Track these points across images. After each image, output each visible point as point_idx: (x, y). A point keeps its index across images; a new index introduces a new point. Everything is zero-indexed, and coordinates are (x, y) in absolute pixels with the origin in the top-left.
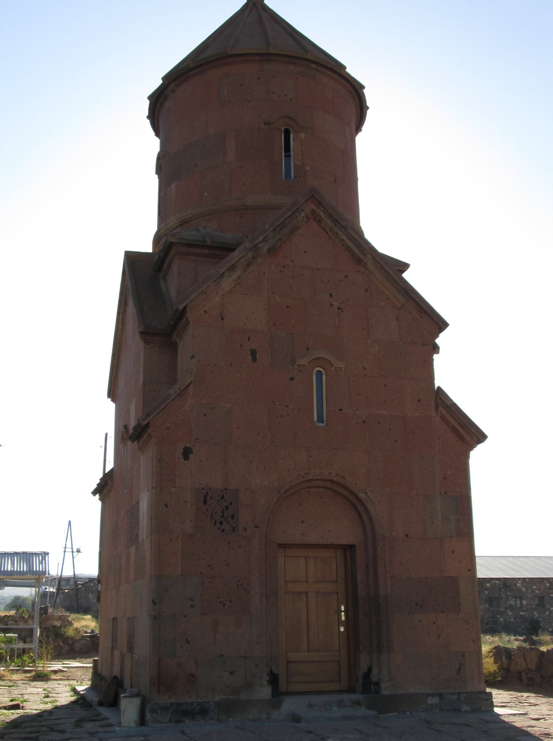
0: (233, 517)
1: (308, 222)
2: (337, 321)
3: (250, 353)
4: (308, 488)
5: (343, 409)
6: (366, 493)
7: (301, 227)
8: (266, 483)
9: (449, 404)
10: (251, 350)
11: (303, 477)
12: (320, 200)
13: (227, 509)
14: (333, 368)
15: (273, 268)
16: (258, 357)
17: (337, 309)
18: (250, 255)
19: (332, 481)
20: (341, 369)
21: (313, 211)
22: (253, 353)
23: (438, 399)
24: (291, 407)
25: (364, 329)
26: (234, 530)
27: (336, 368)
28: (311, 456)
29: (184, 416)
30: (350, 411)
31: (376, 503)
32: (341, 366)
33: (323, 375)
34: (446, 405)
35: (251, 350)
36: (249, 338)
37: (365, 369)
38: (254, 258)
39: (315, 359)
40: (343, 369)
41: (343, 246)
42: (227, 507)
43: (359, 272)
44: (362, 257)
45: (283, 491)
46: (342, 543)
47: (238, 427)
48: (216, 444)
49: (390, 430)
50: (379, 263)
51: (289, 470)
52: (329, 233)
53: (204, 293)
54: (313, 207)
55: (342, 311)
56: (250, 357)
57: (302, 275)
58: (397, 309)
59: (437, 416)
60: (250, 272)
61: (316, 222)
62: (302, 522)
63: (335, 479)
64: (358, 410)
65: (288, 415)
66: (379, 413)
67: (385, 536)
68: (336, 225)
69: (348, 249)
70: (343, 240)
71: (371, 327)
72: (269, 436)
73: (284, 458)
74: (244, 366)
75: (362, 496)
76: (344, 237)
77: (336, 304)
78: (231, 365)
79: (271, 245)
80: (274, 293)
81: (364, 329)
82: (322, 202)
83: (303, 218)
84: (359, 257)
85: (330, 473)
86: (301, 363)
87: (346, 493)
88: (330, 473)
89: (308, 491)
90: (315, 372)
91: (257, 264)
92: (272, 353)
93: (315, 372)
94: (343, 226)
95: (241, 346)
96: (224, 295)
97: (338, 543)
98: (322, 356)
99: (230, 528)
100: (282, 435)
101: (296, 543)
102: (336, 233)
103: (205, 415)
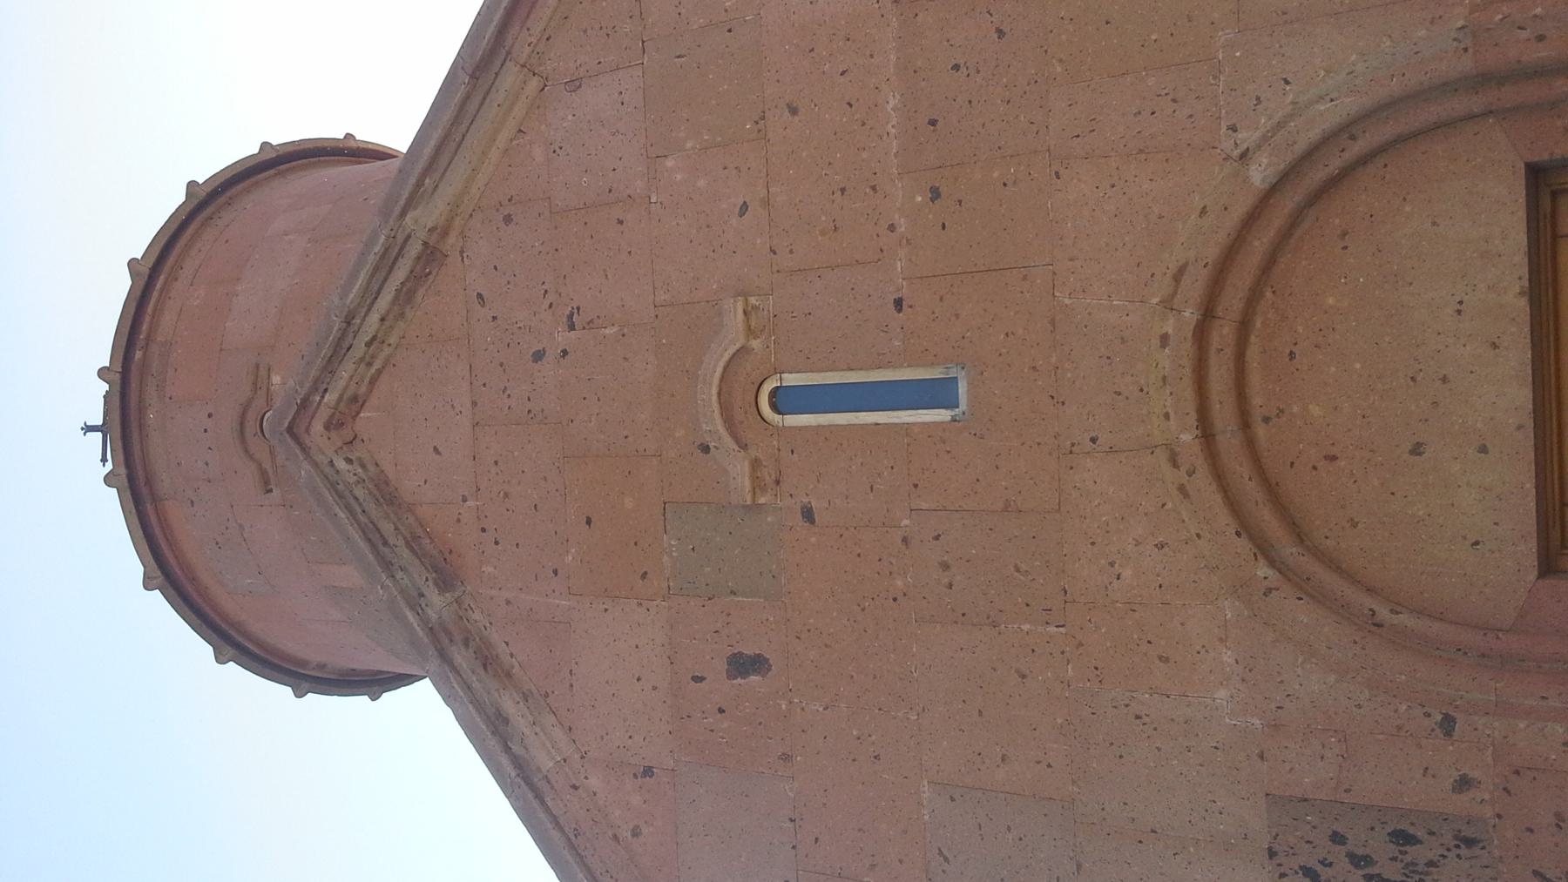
0: (1402, 838)
1: (363, 441)
2: (607, 331)
3: (739, 681)
4: (1245, 424)
6: (1243, 156)
7: (377, 464)
8: (1228, 657)
10: (731, 676)
11: (1190, 473)
13: (1367, 860)
14: (755, 344)
15: (491, 569)
16: (749, 650)
18: (461, 657)
19: (1208, 313)
20: (755, 308)
21: (327, 427)
22: (743, 665)
24: (906, 522)
26: (1470, 842)
27: (750, 332)
28: (1093, 440)
30: (900, 260)
31: (1290, 97)
33: (784, 385)
35: (731, 676)
36: (698, 679)
37: (744, 208)
38: (466, 643)
40: (753, 300)
41: (402, 315)
42: (1356, 860)
43: (462, 252)
44: (415, 248)
45: (1263, 570)
46: (1519, 238)
48: (1079, 866)
49: (956, 67)
51: (1160, 546)
52: (377, 365)
54: (318, 426)
56: (752, 677)
58: (546, 88)
60: (512, 655)
61: (358, 413)
62: (1417, 450)
63: (1190, 315)
64: (892, 228)
65: (937, 538)
67: (1463, 27)
68: (348, 349)
69: (406, 296)
70: (382, 320)
72: (1026, 627)
73: (1112, 564)
74: (784, 707)
75: (1260, 174)
76: (374, 318)
78: (786, 758)
79: (427, 580)
80: (556, 572)
81: (621, 222)
83: (349, 461)
85: (1164, 339)
86: (747, 483)
87: (1259, 244)
88: (1164, 339)
89: (1266, 420)
90: (775, 418)
92: (733, 593)
93: (775, 418)
95: (721, 711)
96: (582, 757)
97: (1520, 259)
98: (715, 398)
99: (1459, 856)
100: (1018, 570)
101: (1530, 486)
102: (368, 345)
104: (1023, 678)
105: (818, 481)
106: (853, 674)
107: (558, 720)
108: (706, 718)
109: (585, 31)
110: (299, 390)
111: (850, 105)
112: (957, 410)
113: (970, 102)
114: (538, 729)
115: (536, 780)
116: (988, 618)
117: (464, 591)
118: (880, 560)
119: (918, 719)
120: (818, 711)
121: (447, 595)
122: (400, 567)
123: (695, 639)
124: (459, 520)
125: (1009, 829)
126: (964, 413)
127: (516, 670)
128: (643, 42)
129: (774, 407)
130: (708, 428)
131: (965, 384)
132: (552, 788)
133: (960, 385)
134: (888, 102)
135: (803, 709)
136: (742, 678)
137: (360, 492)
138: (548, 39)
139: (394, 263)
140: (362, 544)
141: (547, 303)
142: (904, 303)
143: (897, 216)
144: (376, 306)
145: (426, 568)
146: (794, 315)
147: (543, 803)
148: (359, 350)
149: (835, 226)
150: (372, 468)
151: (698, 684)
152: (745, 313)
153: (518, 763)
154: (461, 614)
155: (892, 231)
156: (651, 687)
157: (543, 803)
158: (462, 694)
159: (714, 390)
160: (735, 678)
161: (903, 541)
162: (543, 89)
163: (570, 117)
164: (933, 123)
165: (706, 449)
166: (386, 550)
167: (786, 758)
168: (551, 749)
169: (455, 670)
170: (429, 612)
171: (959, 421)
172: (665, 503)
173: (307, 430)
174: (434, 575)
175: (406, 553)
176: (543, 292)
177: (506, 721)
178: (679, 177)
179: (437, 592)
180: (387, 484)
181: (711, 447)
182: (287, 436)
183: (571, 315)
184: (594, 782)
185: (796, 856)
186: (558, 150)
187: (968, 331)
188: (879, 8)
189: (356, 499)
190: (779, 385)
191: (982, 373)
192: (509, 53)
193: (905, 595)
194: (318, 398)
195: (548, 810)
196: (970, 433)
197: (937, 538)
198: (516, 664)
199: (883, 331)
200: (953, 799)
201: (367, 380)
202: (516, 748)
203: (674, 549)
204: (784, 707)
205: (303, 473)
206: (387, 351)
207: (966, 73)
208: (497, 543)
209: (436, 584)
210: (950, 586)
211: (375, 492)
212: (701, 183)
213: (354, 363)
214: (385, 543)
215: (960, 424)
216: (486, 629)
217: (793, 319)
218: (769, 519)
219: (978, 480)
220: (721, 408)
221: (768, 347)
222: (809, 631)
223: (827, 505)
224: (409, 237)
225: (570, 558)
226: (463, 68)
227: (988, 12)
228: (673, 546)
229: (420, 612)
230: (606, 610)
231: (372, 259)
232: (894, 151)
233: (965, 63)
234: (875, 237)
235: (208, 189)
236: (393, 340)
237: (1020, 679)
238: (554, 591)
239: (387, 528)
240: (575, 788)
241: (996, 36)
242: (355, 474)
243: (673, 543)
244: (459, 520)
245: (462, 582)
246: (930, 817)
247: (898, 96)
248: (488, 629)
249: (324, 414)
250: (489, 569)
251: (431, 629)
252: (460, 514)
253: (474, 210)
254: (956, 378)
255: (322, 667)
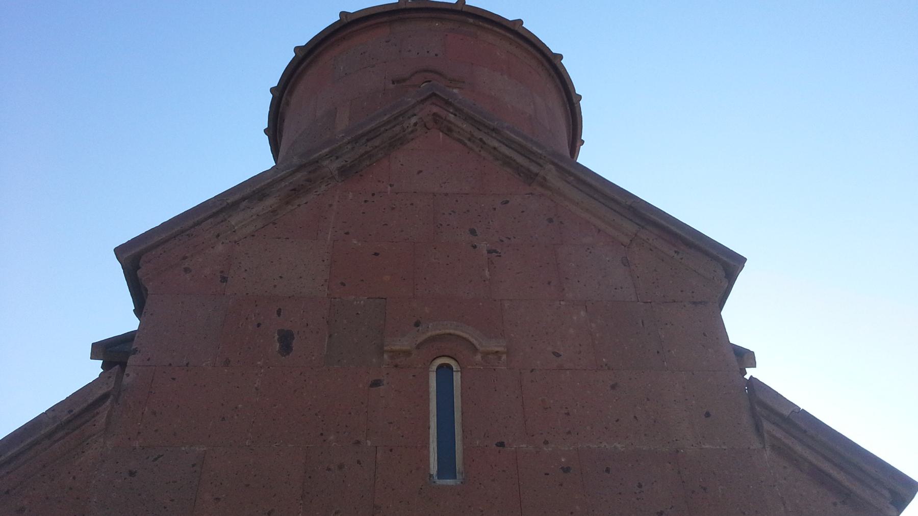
1: (426, 133)
3: (277, 337)
5: (506, 443)
7: (412, 139)
9: (786, 413)
12: (447, 99)
14: (478, 357)
16: (295, 344)
17: (486, 252)
18: (300, 176)
20: (500, 358)
21: (435, 114)
22: (286, 340)
23: (758, 409)
24: (369, 443)
25: (549, 283)
27: (486, 354)
29: (74, 478)
30: (527, 447)
32: (497, 349)
33: (454, 373)
34: (781, 416)
35: (280, 332)
36: (279, 312)
37: (557, 355)
38: (309, 180)
39: (433, 339)
40: (504, 357)
43: (531, 194)
44: (534, 168)
47: (218, 499)
49: (640, 486)
50: (571, 174)
53: (187, 235)
54: (435, 109)
55: (497, 256)
56: (278, 345)
57: (412, 204)
58: (623, 247)
59: (764, 447)
60: (299, 205)
61: (442, 132)
64: (546, 443)
65: (359, 462)
66: (605, 446)
68: (478, 129)
69: (507, 162)
70: (495, 148)
71: (567, 278)
74: (259, 363)
76: (496, 144)
77: (483, 247)
78: (227, 363)
79: (346, 161)
80: (347, 233)
82: (450, 100)
83: (415, 124)
84: (529, 170)
86: (397, 348)
90: (434, 367)
91: (318, 193)
92: (330, 336)
93: (434, 367)
94: (494, 130)
95: (259, 325)
96: (235, 242)
98: (448, 331)
102: (481, 140)
103: (132, 474)
104: (268, 514)
105: (396, 391)
106: (277, 407)
107: (259, 229)
108: (255, 316)
109: (655, 270)
110: (456, 101)
111: (617, 421)
112: (436, 478)
113: (620, 493)
114: (254, 217)
115: (224, 214)
116: (308, 493)
117: (338, 182)
118: (346, 426)
119: (246, 446)
120: (255, 383)
121: (337, 172)
122: (354, 147)
123: (304, 312)
124: (379, 181)
125: (172, 500)
126: (434, 482)
127: (290, 207)
128: (650, 302)
129: (440, 367)
130: (430, 326)
131: (452, 484)
132: (219, 223)
133: (451, 480)
134: (619, 443)
135: (257, 374)
136: (278, 338)
137: (398, 129)
138: (651, 250)
139: (526, 157)
140: (368, 128)
141: (504, 239)
142: (502, 448)
143: (553, 446)
144: (501, 144)
145: (353, 161)
146: (495, 381)
147: (210, 217)
148: (478, 135)
149: (547, 408)
150: (412, 136)
151: (276, 312)
152: (497, 352)
153: (234, 206)
154: (325, 179)
155: (544, 442)
156: (276, 284)
157: (210, 217)
158: (279, 176)
159: (452, 331)
160: (279, 334)
161: (357, 440)
162: (623, 245)
163: (608, 259)
164: (608, 470)
165: (417, 324)
166: (364, 140)
167: (227, 363)
168: (242, 224)
169: (294, 172)
170: (327, 162)
171: (430, 479)
172: (386, 299)
173: (433, 104)
174: (349, 166)
175: (362, 151)
176: (509, 237)
177: (260, 200)
178: (575, 318)
179: (339, 166)
180: (401, 144)
181: (418, 328)
182: (431, 93)
183: (497, 252)
184: (220, 248)
185: (165, 366)
186: (589, 251)
187: (485, 487)
188: (673, 441)
189: (394, 127)
190: (454, 370)
191: (458, 495)
192: (643, 227)
193: (325, 441)
194: (451, 111)
195: (206, 219)
196: (422, 486)
197: (359, 462)
198: (294, 208)
199: (485, 434)
200: (194, 465)
201: (460, 137)
202: (244, 204)
203: (358, 302)
204: (259, 363)
205: (410, 99)
206: (477, 149)
207: (637, 492)
208: (366, 201)
209: (342, 167)
210: (329, 469)
211: (398, 137)
212: (571, 331)
213: (470, 132)
214: (368, 140)
215: (428, 480)
216: (316, 192)
217: (493, 381)
218: (374, 360)
219: (393, 490)
220: (441, 335)
221: (476, 364)
222: (305, 381)
223: (381, 395)
224: (541, 166)
225: (355, 242)
226: (634, 202)
227: (672, 507)
228: (360, 302)
229: (328, 156)
230: (323, 261)
231: (529, 145)
232: (591, 446)
233: (643, 492)
234: (540, 432)
235: (558, 65)
236: (483, 153)
237: (267, 512)
238: (336, 232)
239: (377, 142)
240: (218, 236)
241: (659, 511)
242: (408, 127)
243: (362, 302)
244: (379, 181)
245: (343, 181)
246: (183, 451)
247: (622, 450)
248: (315, 194)
249: (443, 113)
250: (351, 196)
251: (317, 162)
252: (383, 182)
253: (555, 202)
254: (456, 479)
255: (288, 104)
